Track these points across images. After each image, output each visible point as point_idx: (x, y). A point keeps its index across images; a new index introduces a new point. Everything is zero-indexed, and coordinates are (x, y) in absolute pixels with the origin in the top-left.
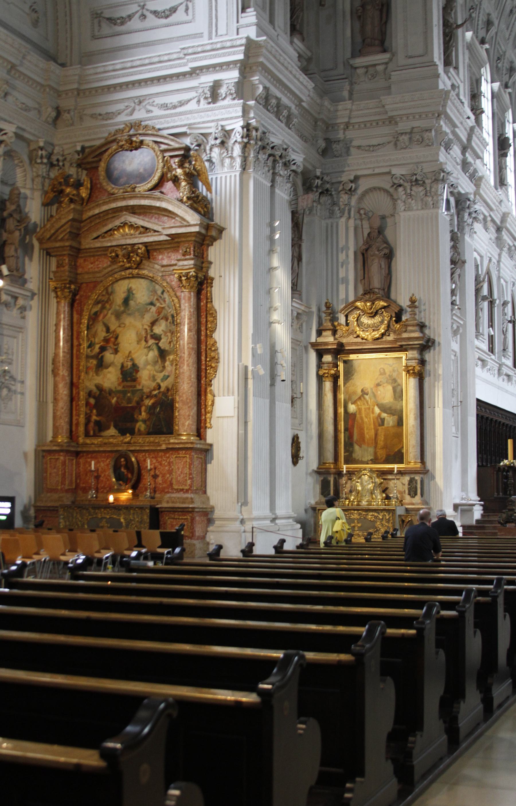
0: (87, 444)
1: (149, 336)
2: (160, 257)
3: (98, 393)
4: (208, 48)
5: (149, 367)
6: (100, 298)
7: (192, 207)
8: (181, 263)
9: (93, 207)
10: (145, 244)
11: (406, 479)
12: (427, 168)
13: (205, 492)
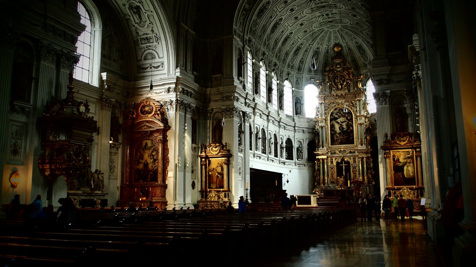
4: (167, 78)
7: (162, 122)
8: (159, 136)
10: (150, 131)
11: (224, 193)
12: (231, 107)
13: (165, 197)
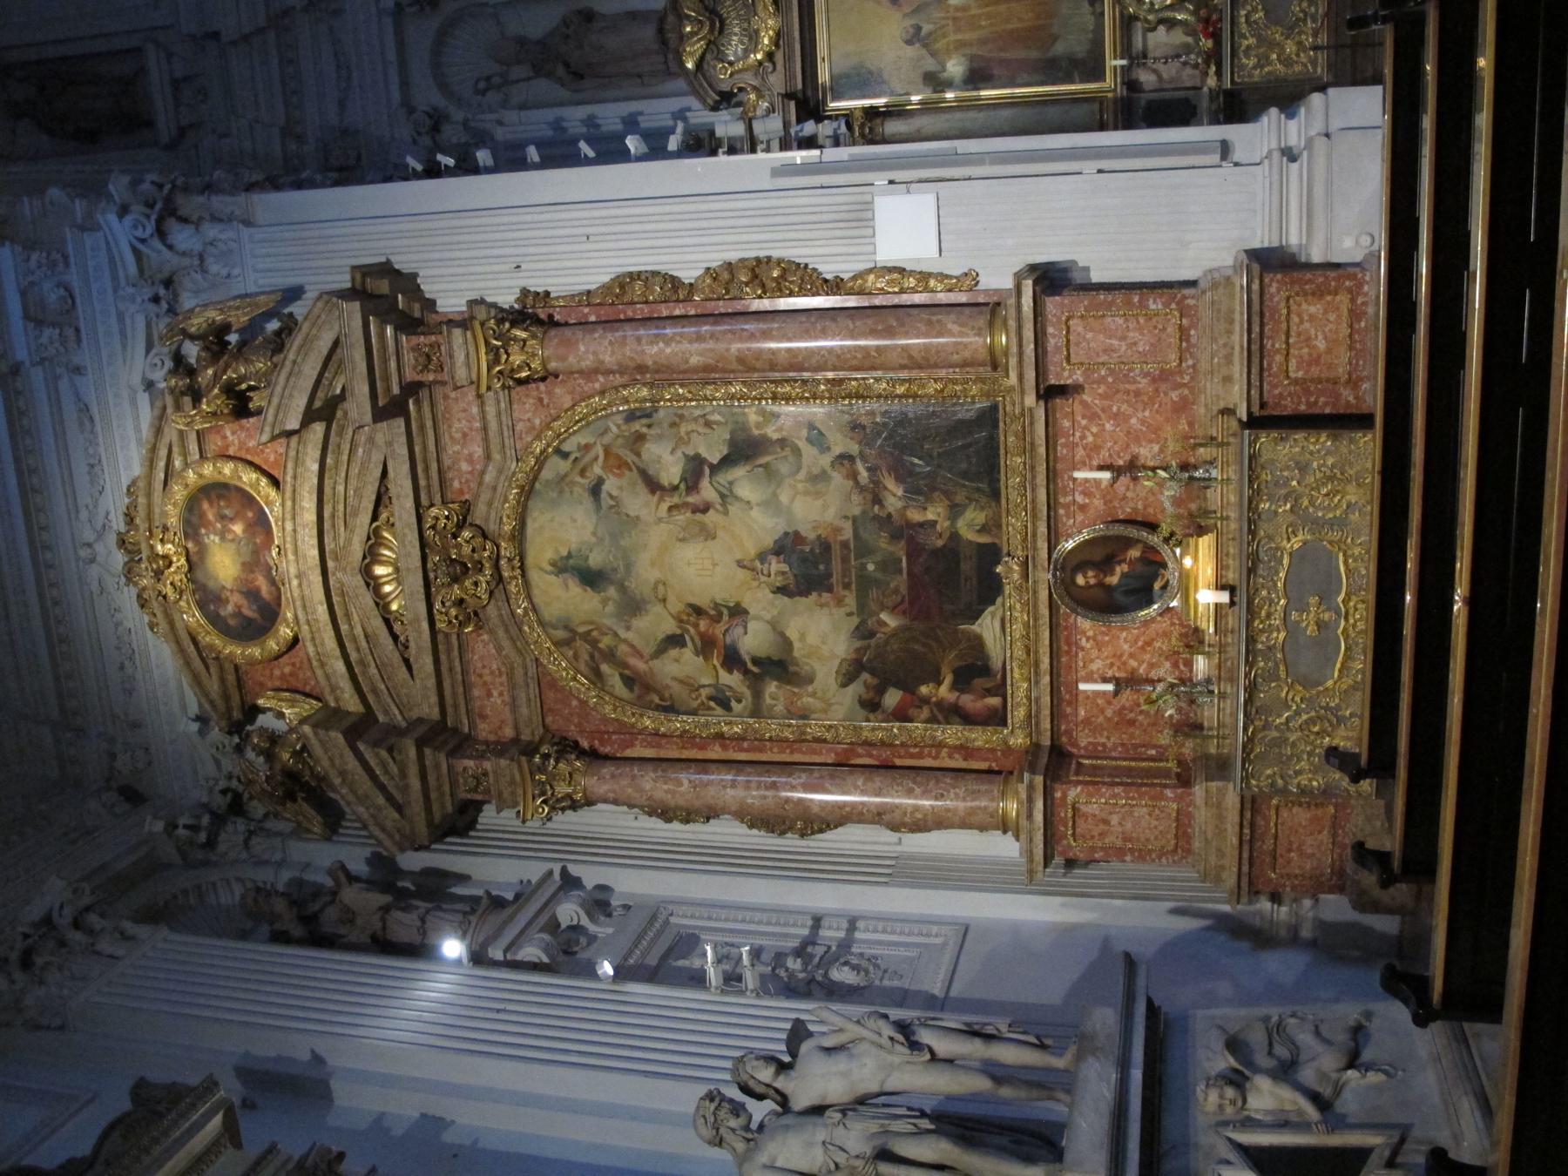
0: (1029, 716)
1: (690, 499)
2: (465, 466)
3: (865, 676)
5: (784, 498)
6: (582, 667)
9: (327, 677)
